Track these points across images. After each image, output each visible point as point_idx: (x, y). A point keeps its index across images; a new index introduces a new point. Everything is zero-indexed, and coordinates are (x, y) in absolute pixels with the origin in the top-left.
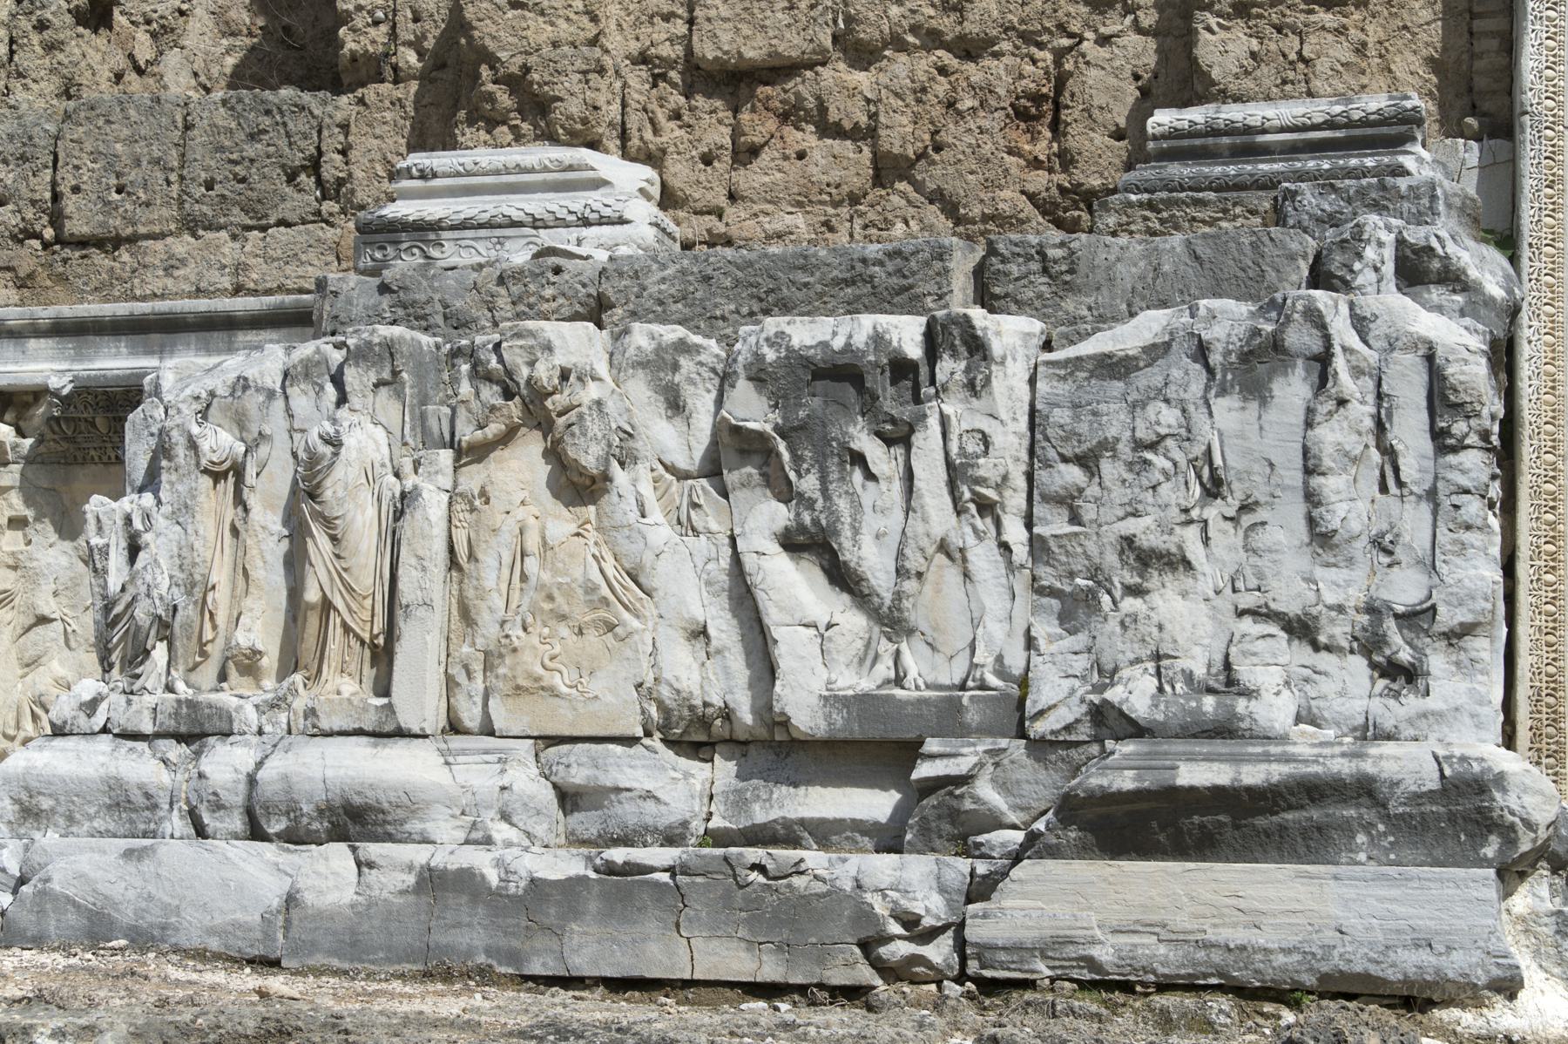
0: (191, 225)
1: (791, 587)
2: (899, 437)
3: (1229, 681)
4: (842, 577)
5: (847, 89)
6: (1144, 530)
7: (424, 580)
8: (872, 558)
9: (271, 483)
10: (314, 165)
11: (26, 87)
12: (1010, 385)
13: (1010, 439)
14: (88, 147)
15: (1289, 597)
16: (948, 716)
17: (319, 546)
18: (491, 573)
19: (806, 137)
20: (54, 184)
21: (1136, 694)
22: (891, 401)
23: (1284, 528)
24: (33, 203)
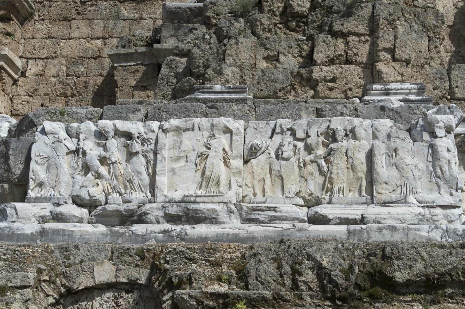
11: (434, 62)
14: (460, 76)
20: (450, 85)
24: (445, 89)
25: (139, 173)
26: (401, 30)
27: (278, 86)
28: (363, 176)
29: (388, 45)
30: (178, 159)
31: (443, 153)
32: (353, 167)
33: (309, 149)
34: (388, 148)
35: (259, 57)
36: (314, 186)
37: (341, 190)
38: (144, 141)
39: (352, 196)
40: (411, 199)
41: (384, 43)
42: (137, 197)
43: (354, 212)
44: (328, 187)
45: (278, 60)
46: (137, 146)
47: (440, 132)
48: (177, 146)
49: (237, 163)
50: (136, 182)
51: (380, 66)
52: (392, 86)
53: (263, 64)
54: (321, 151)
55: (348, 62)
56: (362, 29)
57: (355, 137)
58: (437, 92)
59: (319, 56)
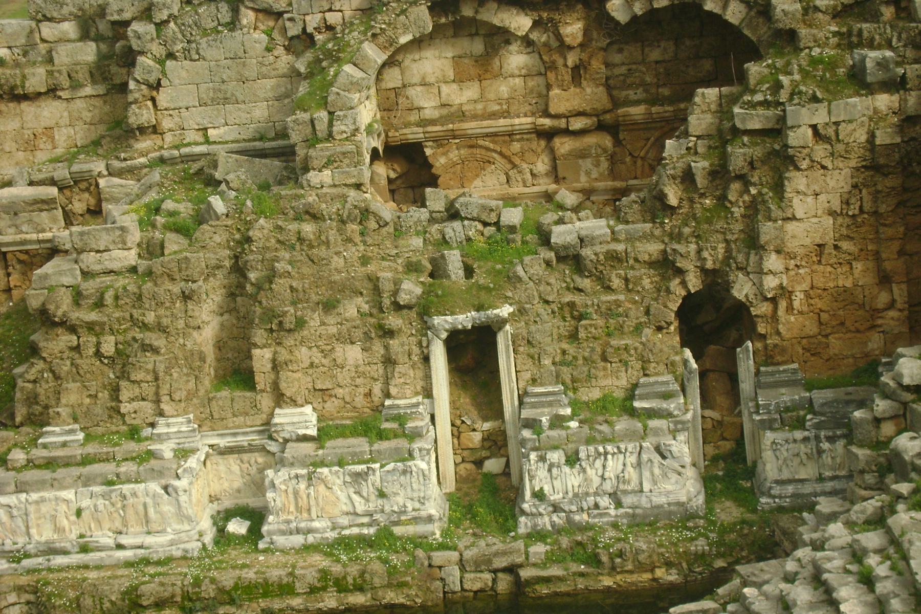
0: (235, 416)
1: (356, 498)
2: (366, 481)
3: (405, 506)
4: (362, 496)
5: (340, 392)
6: (394, 490)
7: (313, 502)
8: (365, 494)
9: (290, 490)
10: (256, 406)
12: (378, 473)
13: (378, 480)
15: (409, 496)
16: (376, 512)
17: (300, 500)
18: (320, 500)
19: (334, 399)
21: (396, 508)
22: (365, 477)
23: (409, 489)
25: (19, 527)
26: (175, 375)
27: (99, 418)
28: (142, 517)
29: (166, 392)
30: (40, 518)
31: (183, 504)
32: (137, 513)
33: (113, 505)
34: (154, 503)
35: (84, 397)
36: (118, 525)
37: (132, 526)
38: (19, 509)
39: (138, 529)
40: (169, 530)
41: (164, 390)
42: (21, 541)
43: (138, 541)
44: (125, 524)
45: (96, 396)
46: (15, 512)
47: (181, 493)
48: (38, 511)
49: (73, 518)
50: (18, 531)
51: (163, 406)
52: (171, 420)
53: (88, 400)
54: (119, 505)
55: (143, 399)
56: (150, 378)
57: (137, 497)
58: (203, 415)
59: (125, 395)
